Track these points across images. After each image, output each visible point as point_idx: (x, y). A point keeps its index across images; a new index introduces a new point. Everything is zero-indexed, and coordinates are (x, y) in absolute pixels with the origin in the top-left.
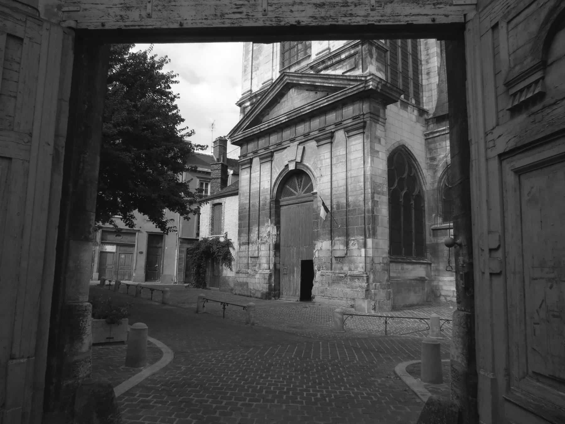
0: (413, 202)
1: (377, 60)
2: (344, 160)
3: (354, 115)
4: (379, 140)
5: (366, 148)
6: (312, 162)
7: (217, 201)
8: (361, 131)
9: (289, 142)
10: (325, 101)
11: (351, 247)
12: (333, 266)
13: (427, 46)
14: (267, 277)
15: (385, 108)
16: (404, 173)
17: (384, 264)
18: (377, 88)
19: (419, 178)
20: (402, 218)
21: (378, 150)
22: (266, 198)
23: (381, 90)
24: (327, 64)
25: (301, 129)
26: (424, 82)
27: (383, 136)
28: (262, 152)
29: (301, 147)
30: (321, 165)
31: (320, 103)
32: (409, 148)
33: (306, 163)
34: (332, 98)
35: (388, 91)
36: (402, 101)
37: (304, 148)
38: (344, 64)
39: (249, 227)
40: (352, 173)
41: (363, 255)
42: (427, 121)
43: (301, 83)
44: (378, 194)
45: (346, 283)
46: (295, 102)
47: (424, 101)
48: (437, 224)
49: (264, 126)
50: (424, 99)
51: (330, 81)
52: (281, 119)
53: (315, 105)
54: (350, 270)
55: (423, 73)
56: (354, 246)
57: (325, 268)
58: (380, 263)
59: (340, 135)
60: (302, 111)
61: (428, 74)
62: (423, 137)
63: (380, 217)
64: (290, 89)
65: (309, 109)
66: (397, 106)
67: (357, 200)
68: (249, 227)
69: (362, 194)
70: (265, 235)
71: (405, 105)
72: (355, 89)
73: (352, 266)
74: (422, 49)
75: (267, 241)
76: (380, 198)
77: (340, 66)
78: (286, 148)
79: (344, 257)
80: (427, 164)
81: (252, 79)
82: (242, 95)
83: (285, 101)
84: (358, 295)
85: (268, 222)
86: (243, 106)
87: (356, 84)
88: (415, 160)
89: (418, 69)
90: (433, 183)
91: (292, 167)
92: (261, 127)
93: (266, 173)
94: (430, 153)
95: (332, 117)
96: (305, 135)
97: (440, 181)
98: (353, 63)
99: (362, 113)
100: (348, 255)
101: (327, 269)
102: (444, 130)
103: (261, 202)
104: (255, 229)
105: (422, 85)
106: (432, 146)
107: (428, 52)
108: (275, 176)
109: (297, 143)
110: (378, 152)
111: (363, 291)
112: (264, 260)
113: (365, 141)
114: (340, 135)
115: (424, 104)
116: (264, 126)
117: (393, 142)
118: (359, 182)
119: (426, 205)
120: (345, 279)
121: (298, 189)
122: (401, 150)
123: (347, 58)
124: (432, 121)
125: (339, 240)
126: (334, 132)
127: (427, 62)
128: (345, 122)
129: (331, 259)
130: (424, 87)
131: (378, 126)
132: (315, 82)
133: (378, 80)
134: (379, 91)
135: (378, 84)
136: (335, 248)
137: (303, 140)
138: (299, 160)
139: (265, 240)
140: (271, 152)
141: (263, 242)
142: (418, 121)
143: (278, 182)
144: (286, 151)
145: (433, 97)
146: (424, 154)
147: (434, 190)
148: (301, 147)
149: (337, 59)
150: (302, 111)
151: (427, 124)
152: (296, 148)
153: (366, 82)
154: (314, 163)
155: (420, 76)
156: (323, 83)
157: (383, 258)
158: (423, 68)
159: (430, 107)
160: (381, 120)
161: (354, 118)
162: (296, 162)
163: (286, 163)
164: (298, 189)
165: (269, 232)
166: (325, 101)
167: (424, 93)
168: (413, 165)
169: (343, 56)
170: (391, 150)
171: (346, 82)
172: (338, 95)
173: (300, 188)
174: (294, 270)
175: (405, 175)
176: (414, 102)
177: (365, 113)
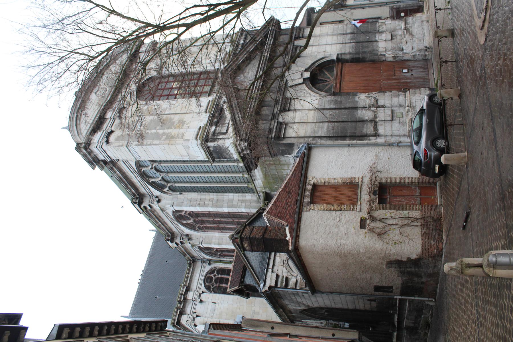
14: (413, 90)
22: (329, 101)
39: (356, 121)
56: (384, 28)
57: (401, 45)
68: (356, 121)
75: (375, 98)
103: (332, 106)
112: (395, 101)
173: (327, 81)
174: (404, 83)
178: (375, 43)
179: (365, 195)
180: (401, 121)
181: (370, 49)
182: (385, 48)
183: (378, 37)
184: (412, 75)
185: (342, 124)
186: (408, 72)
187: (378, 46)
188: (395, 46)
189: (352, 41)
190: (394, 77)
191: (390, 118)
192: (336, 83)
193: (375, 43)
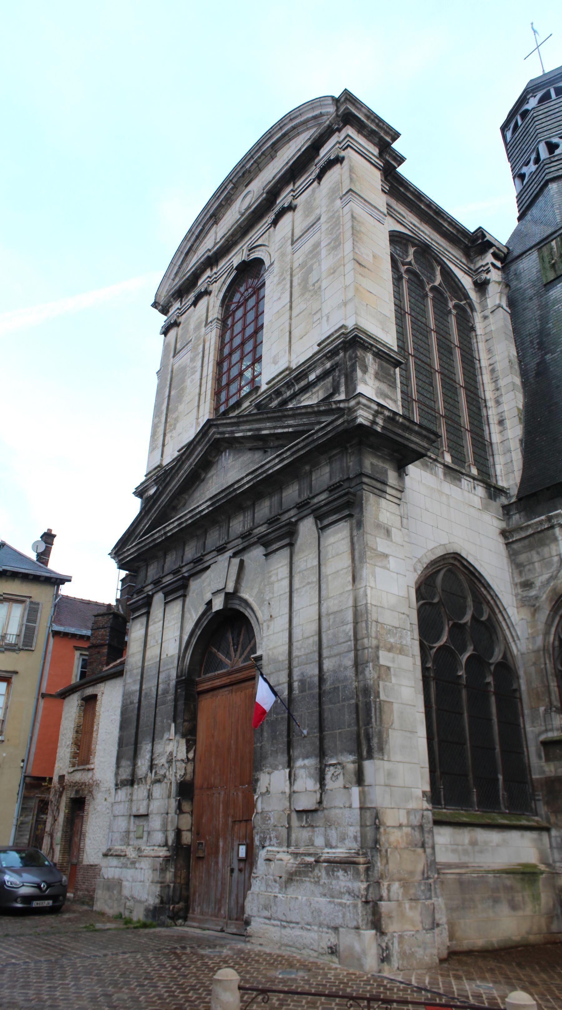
0: (490, 679)
1: (377, 376)
2: (315, 579)
3: (332, 483)
4: (388, 533)
5: (357, 547)
6: (255, 591)
7: (89, 691)
8: (346, 512)
9: (215, 553)
10: (277, 460)
11: (330, 784)
12: (293, 836)
13: (495, 375)
15: (401, 470)
16: (464, 614)
17: (413, 827)
18: (374, 422)
19: (501, 628)
20: (466, 715)
21: (386, 551)
23: (383, 428)
24: (285, 396)
25: (238, 525)
26: (496, 438)
27: (398, 524)
28: (168, 580)
29: (236, 561)
30: (271, 595)
31: (267, 466)
32: (470, 559)
33: (245, 595)
34: (288, 453)
35: (400, 431)
36: (446, 466)
37: (242, 563)
38: (314, 390)
40: (330, 605)
41: (356, 804)
42: (507, 510)
43: (237, 435)
44: (390, 650)
45: (317, 883)
46: (229, 474)
47: (498, 473)
48: (552, 730)
49: (172, 526)
50: (499, 468)
51: (286, 423)
52: (200, 509)
53: (260, 471)
54: (328, 845)
55: (491, 421)
56: (335, 783)
57: (274, 841)
58: (401, 826)
59: (307, 528)
60: (236, 486)
61: (501, 422)
62: (501, 540)
63: (395, 707)
64: (222, 452)
65: (248, 482)
66: (436, 475)
67: (340, 666)
69: (349, 651)
70: (163, 760)
71: (454, 473)
72: (329, 429)
73: (333, 834)
74: (485, 381)
75: (164, 776)
76: (393, 661)
77: (307, 395)
78: (208, 567)
79: (315, 811)
80: (517, 595)
81: (163, 445)
82: (146, 476)
83: (212, 476)
84: (344, 916)
85: (169, 730)
86: (146, 495)
87: (330, 419)
88: (488, 587)
89: (480, 415)
90: (533, 638)
91: (218, 604)
92: (168, 529)
93: (173, 622)
94: (520, 573)
95: (292, 493)
96: (244, 536)
97: (547, 633)
98: (329, 385)
99: (345, 478)
100: (325, 803)
101: (280, 845)
102: (541, 523)
104: (146, 748)
105: (491, 444)
106: (522, 558)
107: (497, 385)
108: (189, 627)
109: (229, 553)
110: (386, 556)
111: (355, 906)
112: (156, 822)
113: (355, 533)
114: (307, 528)
115: (499, 478)
116: (172, 526)
117: (431, 545)
118: (344, 623)
119: (523, 687)
120: (316, 871)
121: (233, 653)
122: (453, 565)
123: (319, 378)
124: (517, 509)
125: (304, 767)
126: (297, 522)
127: (498, 403)
128: (316, 500)
129: (289, 816)
130: (495, 447)
131: (383, 502)
132: (261, 429)
133: (375, 407)
134: (379, 429)
135: (375, 416)
136: (296, 788)
137: (241, 547)
138: (230, 588)
139: (162, 772)
140: (184, 578)
141: (158, 777)
142: (485, 508)
143: (194, 641)
144: (208, 572)
145: (515, 463)
146: (507, 576)
147: (537, 651)
148: (236, 561)
149: (303, 383)
150: (236, 486)
151: (508, 514)
152: (226, 564)
153: (351, 410)
154: (261, 592)
155: (486, 428)
156: (275, 428)
157: (408, 813)
158: (490, 413)
159: (511, 482)
160: (389, 490)
161: (331, 489)
162: (227, 594)
163: (208, 597)
164: (233, 653)
165: (171, 754)
166: (277, 460)
167: (497, 458)
168: (485, 598)
169: (312, 377)
170: (427, 561)
171: (313, 419)
172: (299, 446)
173: (236, 651)
174: (217, 847)
175: (467, 618)
176: (474, 471)
177: (351, 476)
178: (283, 758)
179: (78, 777)
180: (132, 835)
181: (268, 747)
182: (268, 792)
183: (305, 765)
184: (232, 871)
185: (135, 718)
186: (240, 860)
187: (275, 768)
188: (272, 821)
189: (296, 685)
190: (230, 820)
191: (134, 812)
192: (229, 674)
193: (286, 759)
